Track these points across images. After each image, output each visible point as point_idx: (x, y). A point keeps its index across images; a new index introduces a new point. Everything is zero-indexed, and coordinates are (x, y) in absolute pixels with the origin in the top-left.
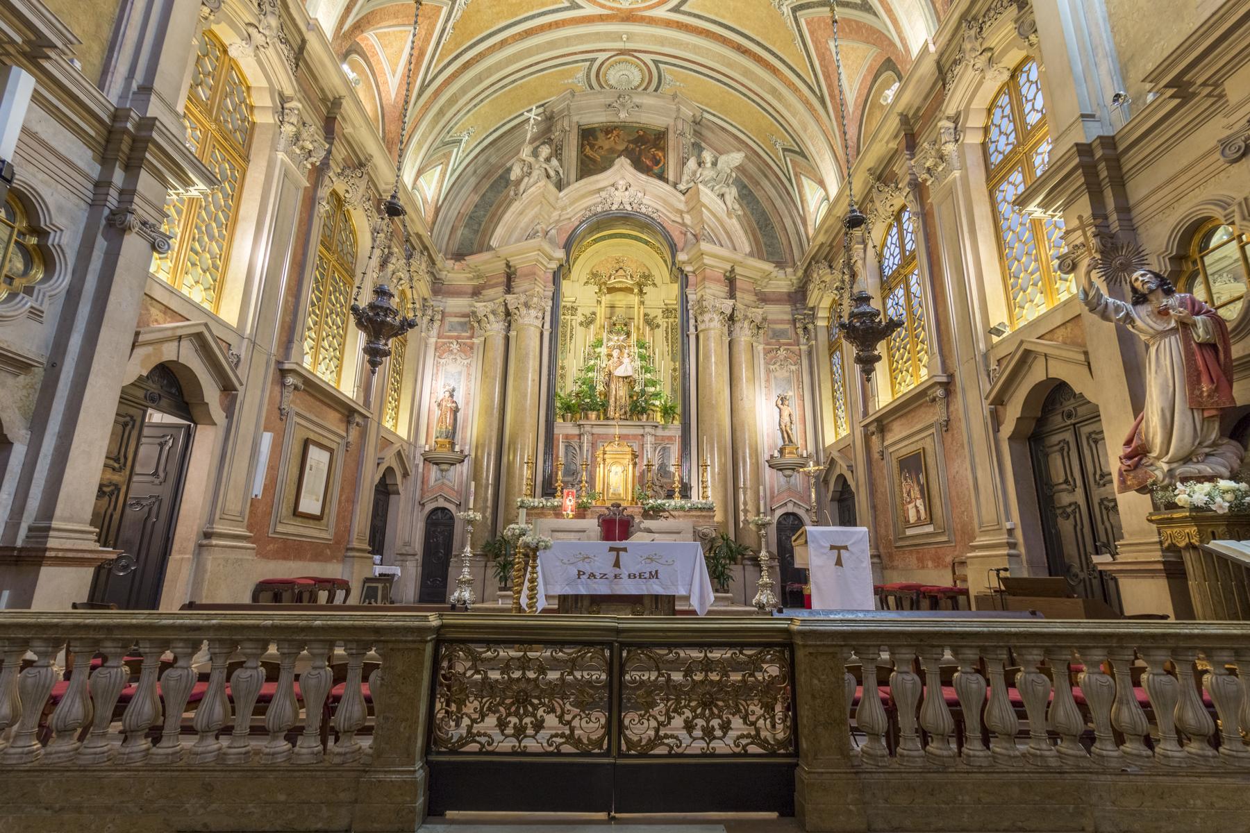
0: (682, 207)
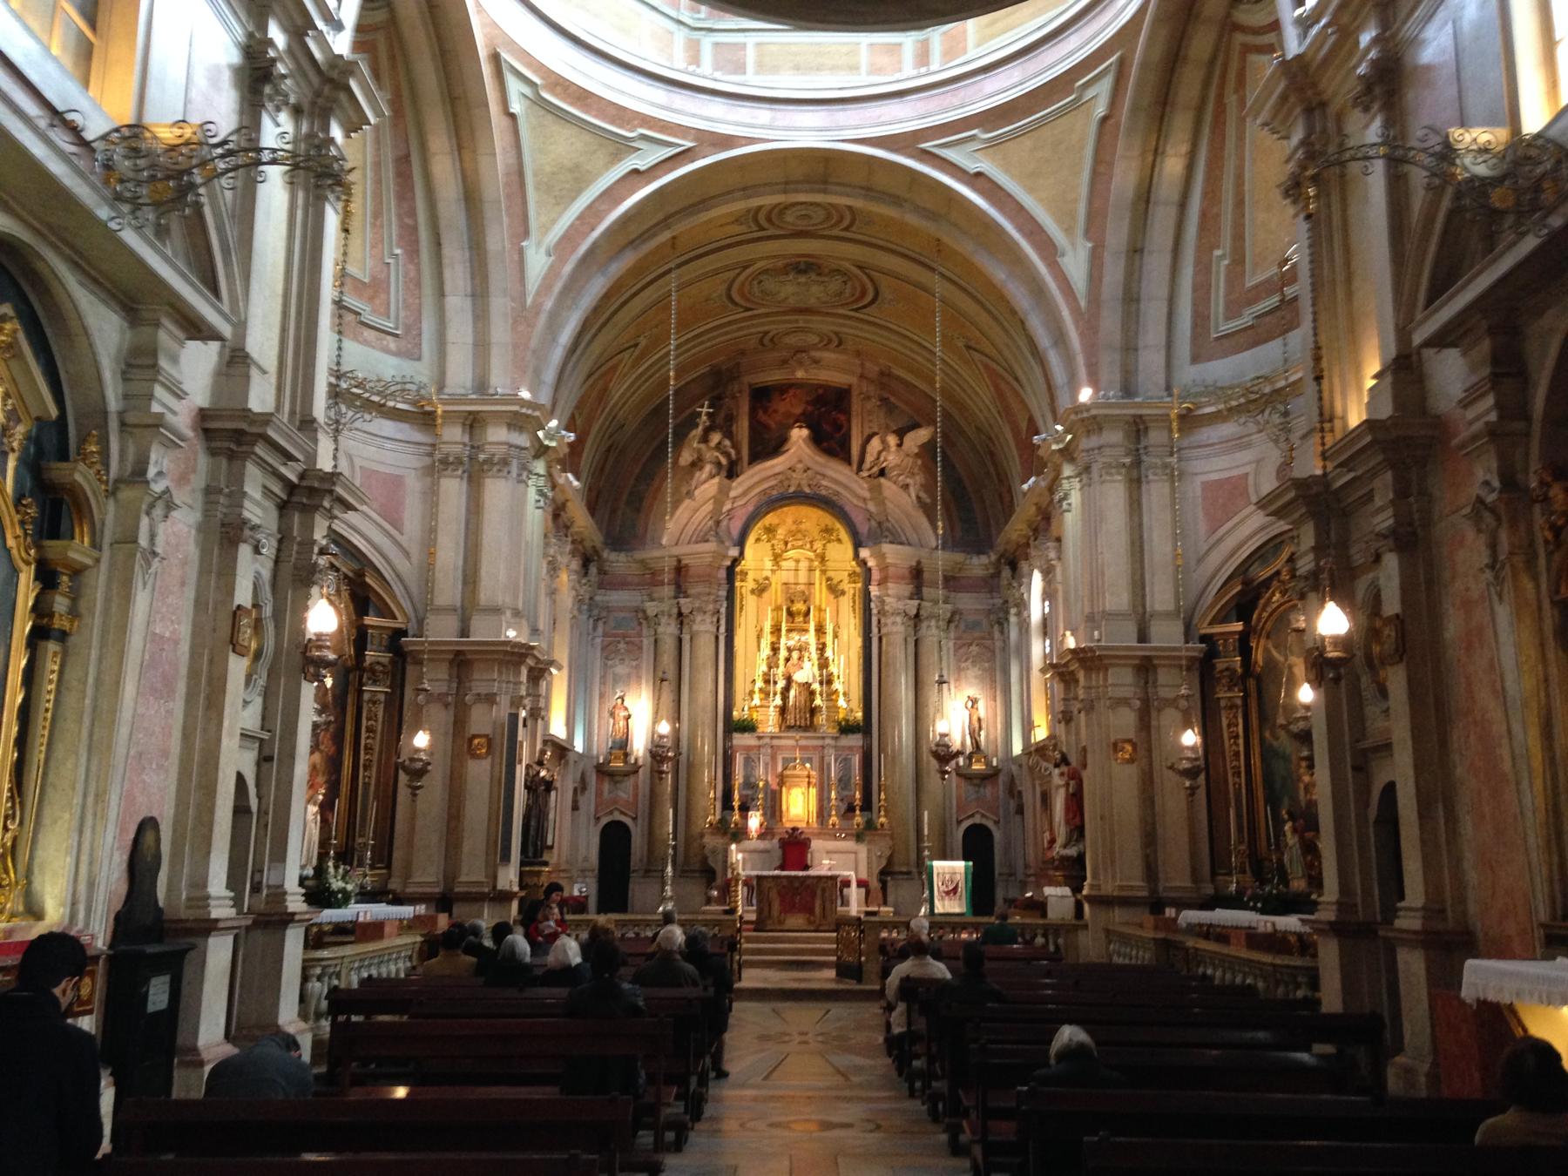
0: (867, 495)
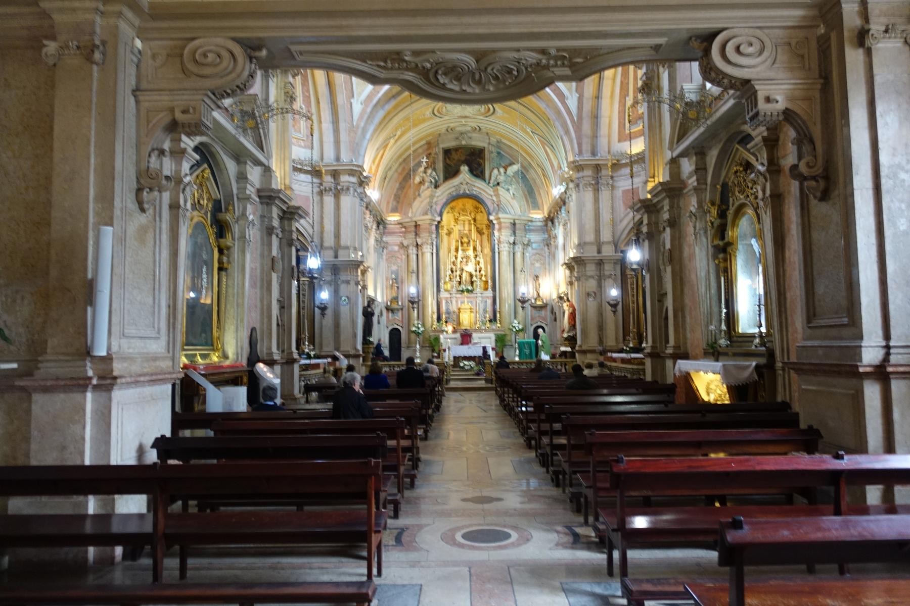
0: (492, 193)
